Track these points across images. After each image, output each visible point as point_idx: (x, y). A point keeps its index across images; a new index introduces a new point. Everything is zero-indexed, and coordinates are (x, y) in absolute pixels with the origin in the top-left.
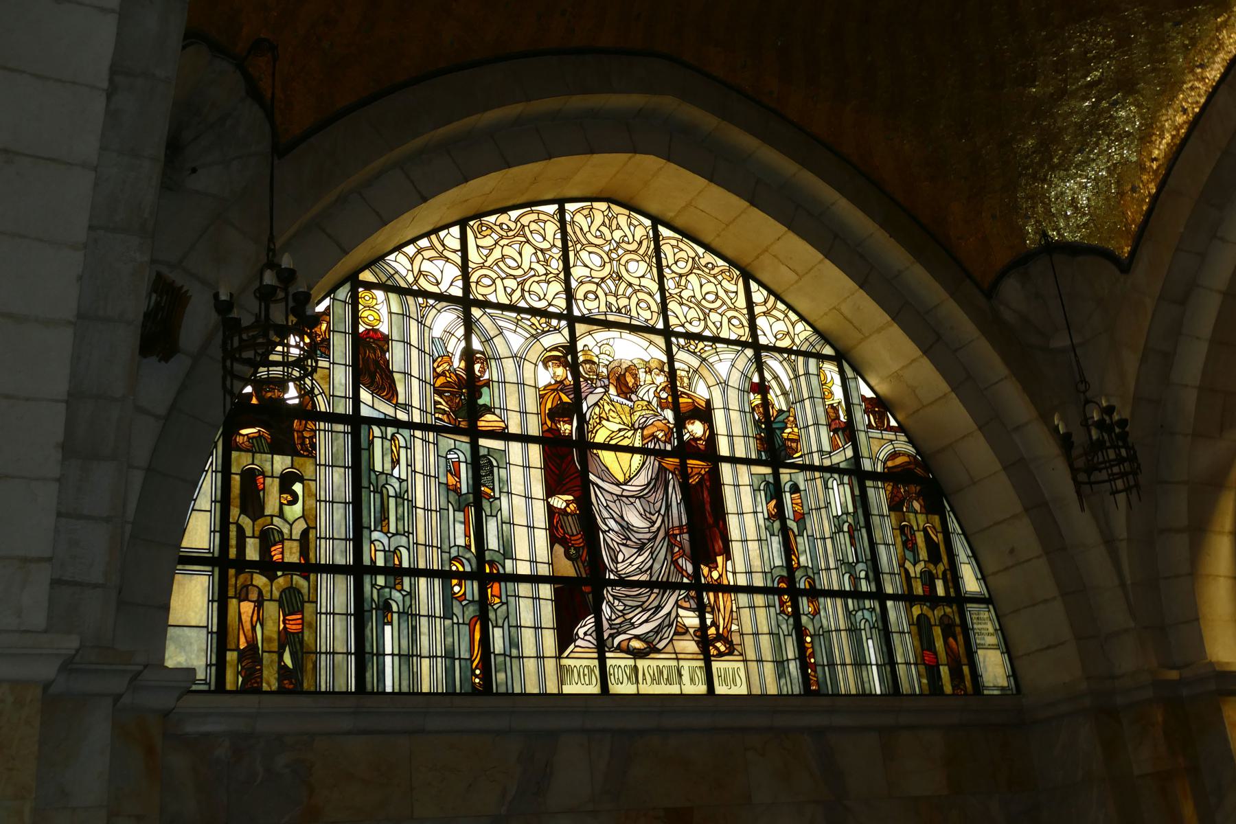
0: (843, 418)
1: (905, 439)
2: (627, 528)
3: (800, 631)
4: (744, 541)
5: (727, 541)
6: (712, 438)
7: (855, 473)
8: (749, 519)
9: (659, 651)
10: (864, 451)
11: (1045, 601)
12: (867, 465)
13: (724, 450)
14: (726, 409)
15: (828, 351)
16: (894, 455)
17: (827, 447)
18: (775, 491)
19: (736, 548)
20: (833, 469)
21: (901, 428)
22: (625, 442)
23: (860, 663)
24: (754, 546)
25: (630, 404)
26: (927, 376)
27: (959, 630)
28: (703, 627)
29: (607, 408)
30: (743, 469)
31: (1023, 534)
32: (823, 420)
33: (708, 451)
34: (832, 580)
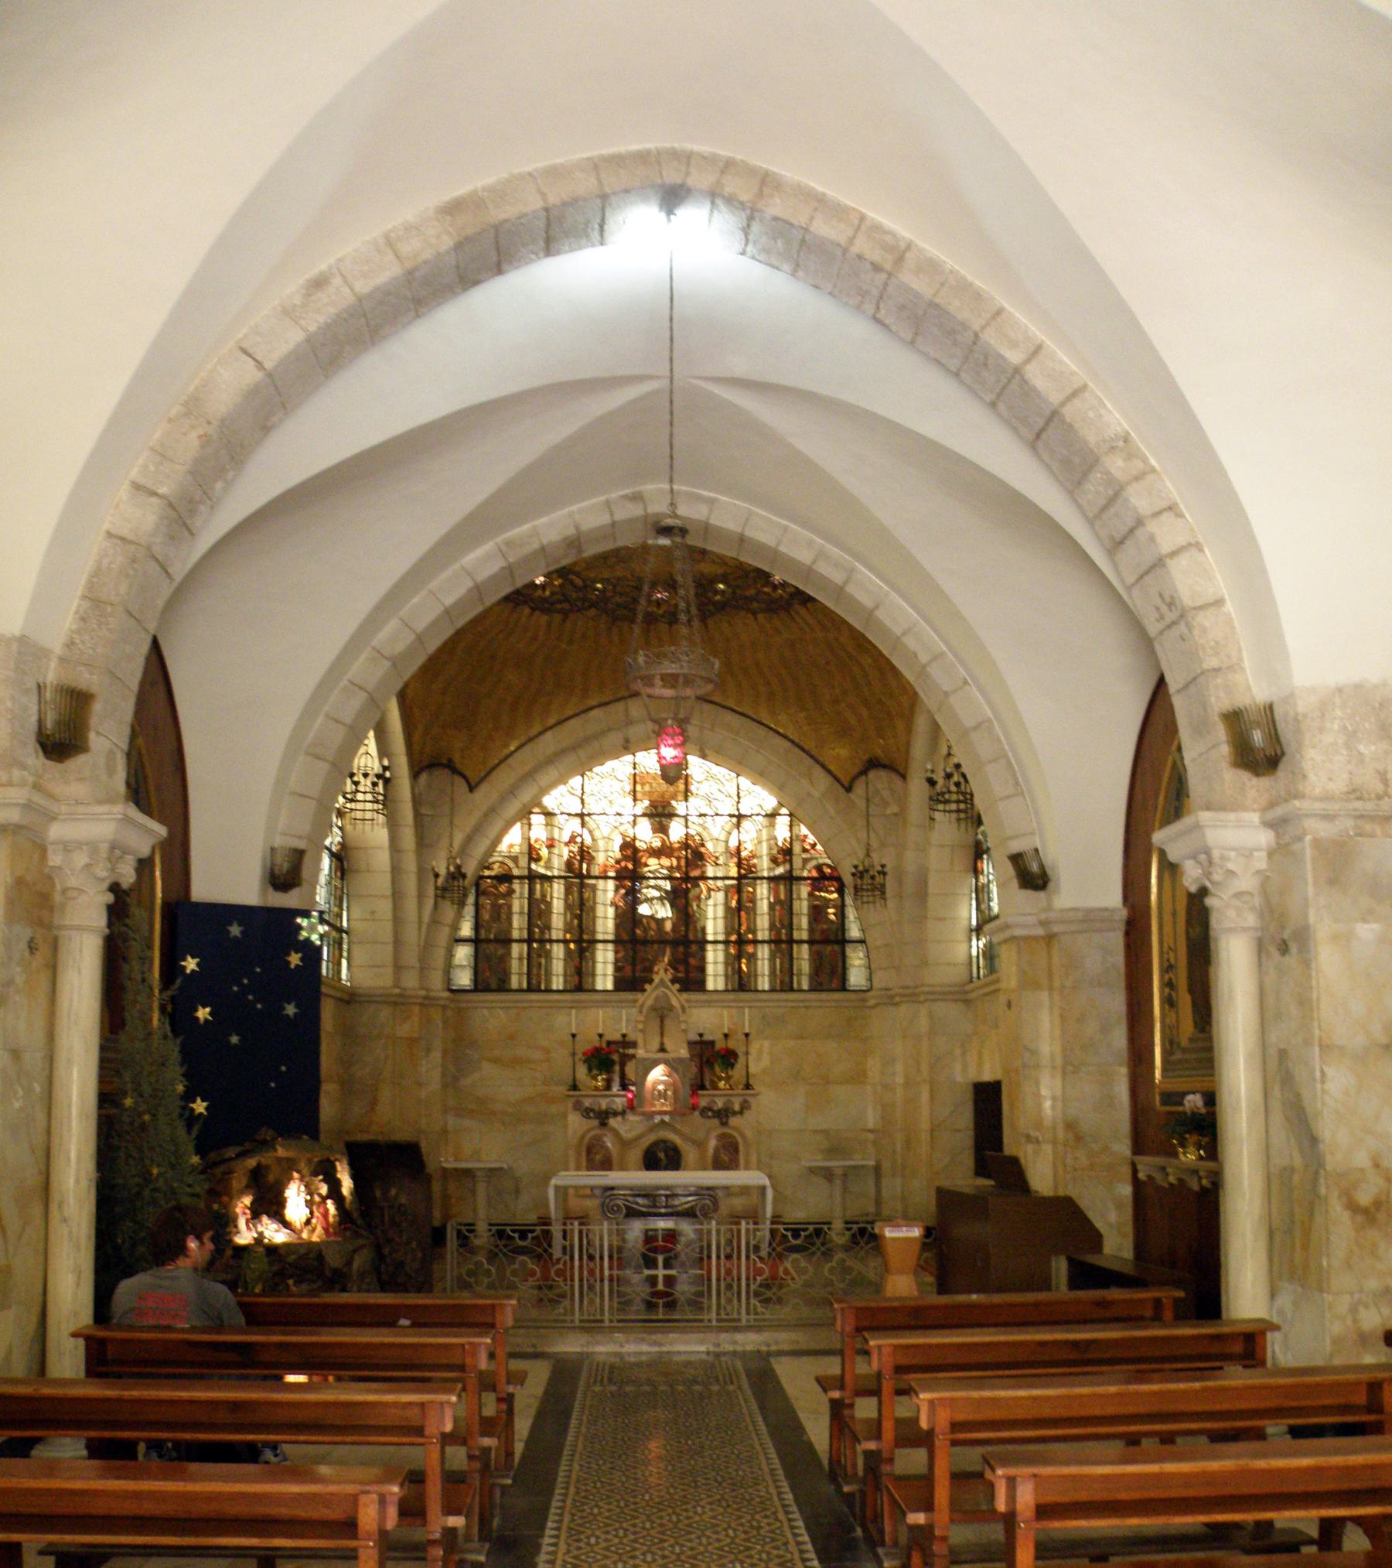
11: (383, 943)
16: (339, 843)
27: (340, 943)
31: (385, 908)
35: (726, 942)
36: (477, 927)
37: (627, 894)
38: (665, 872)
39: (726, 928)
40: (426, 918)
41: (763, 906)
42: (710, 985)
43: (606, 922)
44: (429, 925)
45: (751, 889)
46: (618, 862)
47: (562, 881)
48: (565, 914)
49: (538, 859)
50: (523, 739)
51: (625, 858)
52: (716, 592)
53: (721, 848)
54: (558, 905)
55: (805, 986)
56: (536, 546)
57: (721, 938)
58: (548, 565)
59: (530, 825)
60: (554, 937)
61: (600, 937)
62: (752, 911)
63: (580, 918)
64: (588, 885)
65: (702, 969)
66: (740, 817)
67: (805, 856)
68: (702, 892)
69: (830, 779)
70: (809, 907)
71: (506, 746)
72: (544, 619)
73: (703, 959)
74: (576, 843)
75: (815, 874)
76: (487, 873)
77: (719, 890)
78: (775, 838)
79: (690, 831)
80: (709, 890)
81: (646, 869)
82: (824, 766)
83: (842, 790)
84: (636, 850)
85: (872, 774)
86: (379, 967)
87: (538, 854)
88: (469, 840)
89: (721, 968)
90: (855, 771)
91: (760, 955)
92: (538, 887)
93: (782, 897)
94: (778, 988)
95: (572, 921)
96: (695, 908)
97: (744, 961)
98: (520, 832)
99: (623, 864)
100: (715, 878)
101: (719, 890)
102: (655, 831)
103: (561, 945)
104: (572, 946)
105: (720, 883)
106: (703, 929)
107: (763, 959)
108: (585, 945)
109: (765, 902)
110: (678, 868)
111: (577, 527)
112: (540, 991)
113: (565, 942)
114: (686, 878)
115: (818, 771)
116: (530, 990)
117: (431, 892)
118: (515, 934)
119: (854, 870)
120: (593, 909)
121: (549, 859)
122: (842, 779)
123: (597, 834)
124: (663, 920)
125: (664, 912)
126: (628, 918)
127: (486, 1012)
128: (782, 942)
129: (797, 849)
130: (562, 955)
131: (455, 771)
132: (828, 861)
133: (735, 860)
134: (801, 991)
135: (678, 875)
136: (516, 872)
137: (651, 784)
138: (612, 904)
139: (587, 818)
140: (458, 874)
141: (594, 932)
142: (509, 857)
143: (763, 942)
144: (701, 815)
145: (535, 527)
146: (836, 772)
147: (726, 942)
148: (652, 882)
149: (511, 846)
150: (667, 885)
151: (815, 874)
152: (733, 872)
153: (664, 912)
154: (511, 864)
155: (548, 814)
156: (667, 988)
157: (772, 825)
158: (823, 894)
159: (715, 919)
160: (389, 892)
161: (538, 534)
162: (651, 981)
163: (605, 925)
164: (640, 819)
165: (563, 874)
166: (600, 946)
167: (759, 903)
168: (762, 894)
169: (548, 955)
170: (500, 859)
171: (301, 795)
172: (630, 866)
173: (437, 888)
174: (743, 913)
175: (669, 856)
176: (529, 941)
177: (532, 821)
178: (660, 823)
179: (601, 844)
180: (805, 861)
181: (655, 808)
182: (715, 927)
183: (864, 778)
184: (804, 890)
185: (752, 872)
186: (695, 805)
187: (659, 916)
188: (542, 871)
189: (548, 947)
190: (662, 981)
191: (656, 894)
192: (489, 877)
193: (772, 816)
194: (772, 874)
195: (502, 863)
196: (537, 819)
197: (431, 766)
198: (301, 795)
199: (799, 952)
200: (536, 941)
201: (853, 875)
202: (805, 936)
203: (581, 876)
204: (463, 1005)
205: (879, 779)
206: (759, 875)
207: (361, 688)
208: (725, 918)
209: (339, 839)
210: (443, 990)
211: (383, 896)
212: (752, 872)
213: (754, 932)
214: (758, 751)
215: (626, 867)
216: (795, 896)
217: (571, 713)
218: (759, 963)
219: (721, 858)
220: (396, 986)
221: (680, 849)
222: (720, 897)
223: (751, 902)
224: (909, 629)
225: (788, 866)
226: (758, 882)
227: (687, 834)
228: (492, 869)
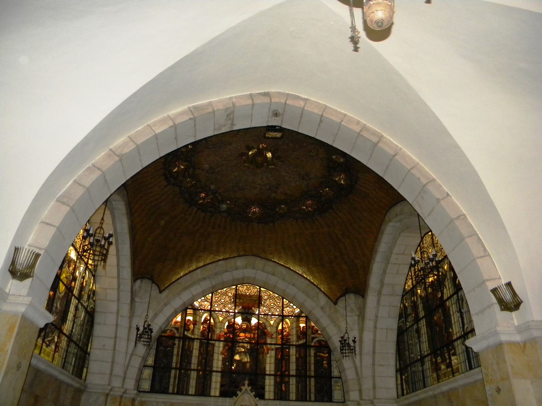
0: (90, 293)
1: (94, 304)
2: (57, 308)
3: (67, 351)
4: (69, 320)
5: (67, 319)
6: (74, 287)
7: (86, 309)
8: (71, 314)
9: (49, 346)
10: (89, 305)
12: (88, 309)
13: (74, 293)
14: (78, 280)
15: (94, 273)
16: (92, 308)
17: (85, 301)
18: (77, 308)
19: (68, 321)
20: (84, 307)
21: (94, 301)
22: (64, 281)
23: (71, 364)
24: (70, 322)
25: (68, 270)
26: (113, 294)
28: (57, 342)
29: (65, 270)
30: (75, 299)
32: (87, 293)
33: (72, 292)
34: (75, 339)
35: (275, 375)
36: (155, 361)
37: (228, 349)
38: (247, 339)
39: (275, 368)
40: (130, 351)
41: (293, 359)
42: (267, 396)
43: (218, 363)
44: (132, 355)
45: (287, 350)
46: (226, 333)
47: (199, 341)
48: (199, 357)
49: (188, 330)
50: (187, 272)
51: (229, 332)
52: (281, 208)
53: (274, 330)
54: (196, 353)
55: (313, 398)
56: (210, 110)
57: (273, 373)
58: (215, 129)
59: (186, 313)
60: (192, 368)
61: (215, 369)
62: (288, 361)
63: (206, 359)
64: (211, 343)
65: (263, 388)
66: (283, 317)
67: (313, 336)
68: (265, 350)
69: (327, 298)
70: (315, 361)
71: (180, 274)
72: (203, 214)
73: (264, 383)
74: (207, 323)
75: (317, 344)
76: (163, 334)
77: (272, 350)
78: (300, 327)
79: (261, 322)
80: (268, 349)
81: (239, 338)
82: (324, 293)
83: (332, 304)
84: (235, 329)
85: (347, 296)
86: (102, 374)
87: (189, 327)
88: (156, 315)
89: (272, 388)
90: (339, 294)
91: (291, 382)
92: (187, 343)
93: (302, 355)
94: (300, 399)
95: (202, 360)
96: (261, 357)
97: (283, 385)
98: (180, 316)
99: (228, 335)
100: (271, 344)
101: (273, 350)
102: (243, 320)
103: (196, 372)
104: (201, 373)
105: (273, 347)
106: (265, 368)
107: (293, 384)
108: (207, 373)
109: (294, 357)
110: (254, 338)
111: (234, 105)
112: (182, 394)
113: (198, 371)
114: (257, 343)
115: (321, 295)
116: (178, 393)
117: (133, 337)
118: (174, 365)
119: (341, 339)
120: (212, 356)
121: (193, 330)
122: (332, 298)
123: (217, 320)
124: (245, 363)
125: (246, 359)
126: (229, 359)
127: (154, 403)
128: (302, 376)
129: (309, 332)
130: (195, 377)
131: (153, 282)
132: (323, 339)
133: (280, 336)
134: (310, 401)
135: (254, 342)
136: (177, 335)
137: (243, 299)
138: (221, 353)
139: (213, 313)
140: (148, 329)
141: (212, 366)
142: (175, 328)
143: (293, 376)
144: (265, 315)
145: (211, 102)
146: (330, 296)
147: (275, 375)
148: (241, 344)
149: (176, 322)
150: (248, 346)
151: (317, 344)
152: (280, 342)
153: (246, 359)
154: (175, 331)
155: (195, 309)
156: (249, 394)
157: (298, 322)
158: (321, 354)
159: (270, 363)
160: (113, 336)
161: (212, 106)
162: (241, 390)
163: (217, 363)
164: (237, 315)
165: (199, 337)
166: (214, 374)
167: (291, 357)
168: (293, 352)
169: (189, 376)
170: (170, 328)
171: (48, 224)
172: (231, 336)
173: (137, 334)
174: (283, 362)
175: (250, 332)
176: (180, 369)
177: (188, 312)
178: (247, 317)
179: (218, 325)
180: (313, 338)
181: (245, 310)
182: (270, 367)
183: (343, 298)
184: (312, 352)
185: (288, 342)
186: (263, 309)
187: (244, 361)
188: (190, 335)
189: (189, 372)
190: (246, 389)
191: (243, 350)
192: (164, 336)
193: (298, 316)
194: (297, 344)
195: (171, 330)
196: (189, 311)
197: (142, 278)
198: (48, 224)
199: (310, 381)
200: (184, 370)
201: (340, 341)
202: (313, 374)
203: (208, 339)
204: (143, 399)
205: (351, 299)
206: (292, 343)
207: (99, 169)
208: (275, 363)
209: (92, 306)
210: (134, 389)
211: (111, 338)
212: (288, 342)
213: (289, 371)
214: (294, 285)
215: (229, 336)
216: (308, 355)
217: (210, 261)
218: (291, 386)
219: (274, 335)
220: (109, 385)
221: (255, 329)
222: (273, 353)
223: (287, 356)
224: (414, 167)
225: (304, 341)
226: (291, 347)
227: (258, 322)
228: (166, 333)
